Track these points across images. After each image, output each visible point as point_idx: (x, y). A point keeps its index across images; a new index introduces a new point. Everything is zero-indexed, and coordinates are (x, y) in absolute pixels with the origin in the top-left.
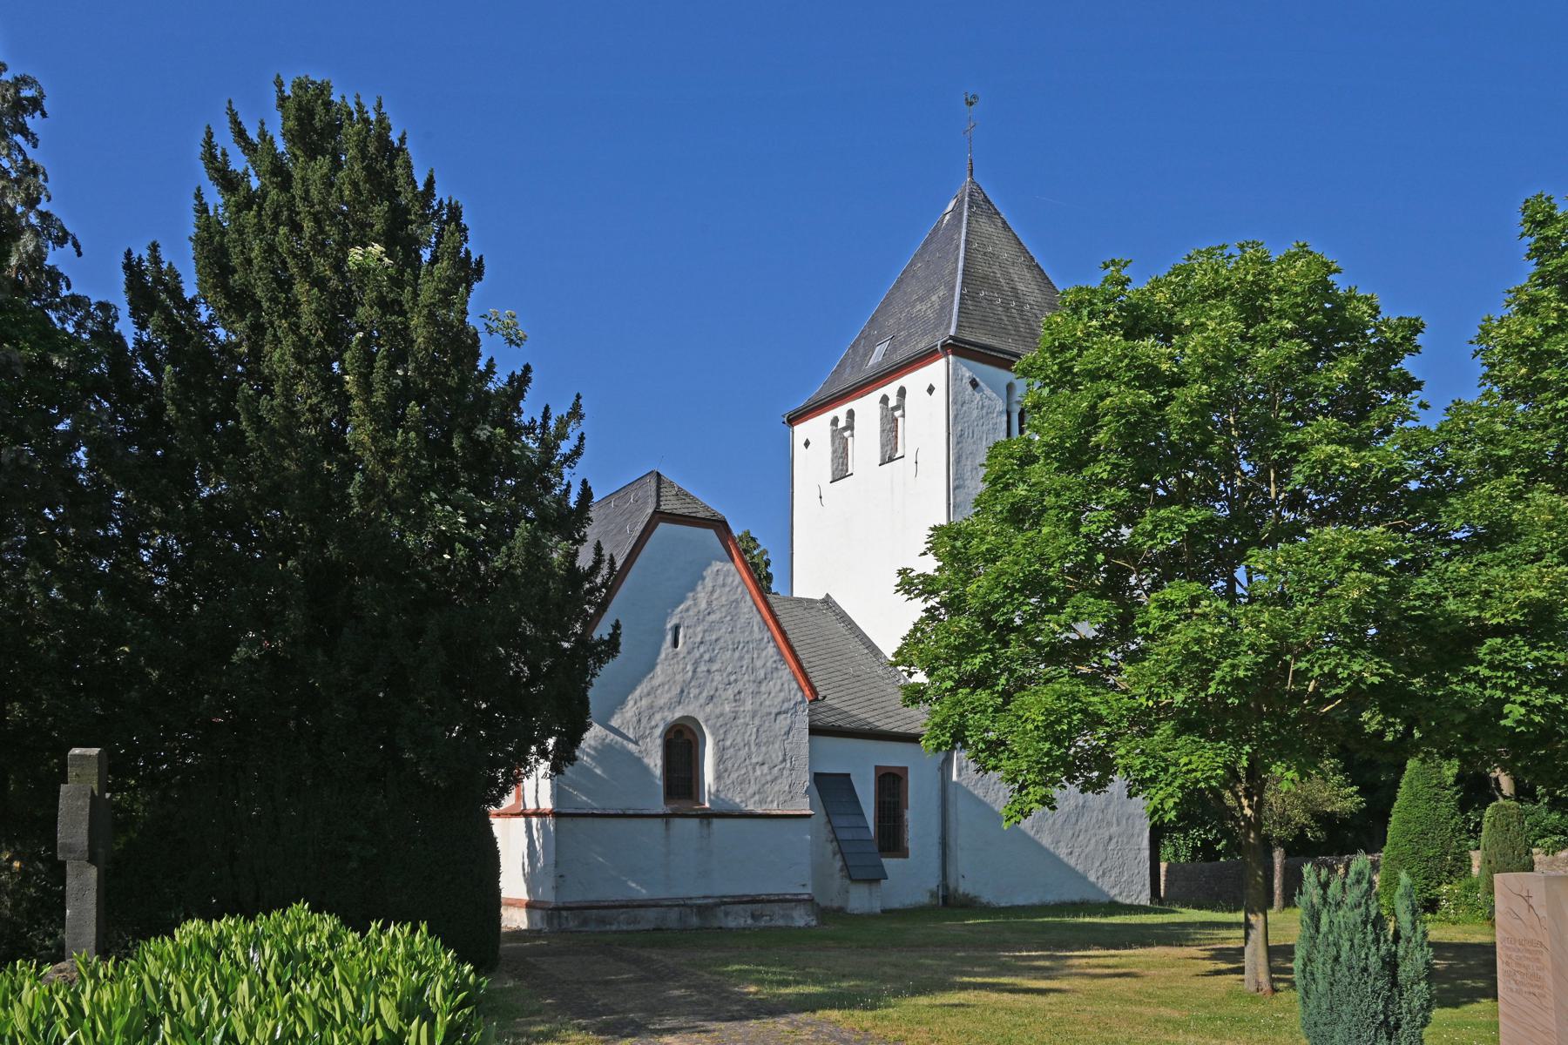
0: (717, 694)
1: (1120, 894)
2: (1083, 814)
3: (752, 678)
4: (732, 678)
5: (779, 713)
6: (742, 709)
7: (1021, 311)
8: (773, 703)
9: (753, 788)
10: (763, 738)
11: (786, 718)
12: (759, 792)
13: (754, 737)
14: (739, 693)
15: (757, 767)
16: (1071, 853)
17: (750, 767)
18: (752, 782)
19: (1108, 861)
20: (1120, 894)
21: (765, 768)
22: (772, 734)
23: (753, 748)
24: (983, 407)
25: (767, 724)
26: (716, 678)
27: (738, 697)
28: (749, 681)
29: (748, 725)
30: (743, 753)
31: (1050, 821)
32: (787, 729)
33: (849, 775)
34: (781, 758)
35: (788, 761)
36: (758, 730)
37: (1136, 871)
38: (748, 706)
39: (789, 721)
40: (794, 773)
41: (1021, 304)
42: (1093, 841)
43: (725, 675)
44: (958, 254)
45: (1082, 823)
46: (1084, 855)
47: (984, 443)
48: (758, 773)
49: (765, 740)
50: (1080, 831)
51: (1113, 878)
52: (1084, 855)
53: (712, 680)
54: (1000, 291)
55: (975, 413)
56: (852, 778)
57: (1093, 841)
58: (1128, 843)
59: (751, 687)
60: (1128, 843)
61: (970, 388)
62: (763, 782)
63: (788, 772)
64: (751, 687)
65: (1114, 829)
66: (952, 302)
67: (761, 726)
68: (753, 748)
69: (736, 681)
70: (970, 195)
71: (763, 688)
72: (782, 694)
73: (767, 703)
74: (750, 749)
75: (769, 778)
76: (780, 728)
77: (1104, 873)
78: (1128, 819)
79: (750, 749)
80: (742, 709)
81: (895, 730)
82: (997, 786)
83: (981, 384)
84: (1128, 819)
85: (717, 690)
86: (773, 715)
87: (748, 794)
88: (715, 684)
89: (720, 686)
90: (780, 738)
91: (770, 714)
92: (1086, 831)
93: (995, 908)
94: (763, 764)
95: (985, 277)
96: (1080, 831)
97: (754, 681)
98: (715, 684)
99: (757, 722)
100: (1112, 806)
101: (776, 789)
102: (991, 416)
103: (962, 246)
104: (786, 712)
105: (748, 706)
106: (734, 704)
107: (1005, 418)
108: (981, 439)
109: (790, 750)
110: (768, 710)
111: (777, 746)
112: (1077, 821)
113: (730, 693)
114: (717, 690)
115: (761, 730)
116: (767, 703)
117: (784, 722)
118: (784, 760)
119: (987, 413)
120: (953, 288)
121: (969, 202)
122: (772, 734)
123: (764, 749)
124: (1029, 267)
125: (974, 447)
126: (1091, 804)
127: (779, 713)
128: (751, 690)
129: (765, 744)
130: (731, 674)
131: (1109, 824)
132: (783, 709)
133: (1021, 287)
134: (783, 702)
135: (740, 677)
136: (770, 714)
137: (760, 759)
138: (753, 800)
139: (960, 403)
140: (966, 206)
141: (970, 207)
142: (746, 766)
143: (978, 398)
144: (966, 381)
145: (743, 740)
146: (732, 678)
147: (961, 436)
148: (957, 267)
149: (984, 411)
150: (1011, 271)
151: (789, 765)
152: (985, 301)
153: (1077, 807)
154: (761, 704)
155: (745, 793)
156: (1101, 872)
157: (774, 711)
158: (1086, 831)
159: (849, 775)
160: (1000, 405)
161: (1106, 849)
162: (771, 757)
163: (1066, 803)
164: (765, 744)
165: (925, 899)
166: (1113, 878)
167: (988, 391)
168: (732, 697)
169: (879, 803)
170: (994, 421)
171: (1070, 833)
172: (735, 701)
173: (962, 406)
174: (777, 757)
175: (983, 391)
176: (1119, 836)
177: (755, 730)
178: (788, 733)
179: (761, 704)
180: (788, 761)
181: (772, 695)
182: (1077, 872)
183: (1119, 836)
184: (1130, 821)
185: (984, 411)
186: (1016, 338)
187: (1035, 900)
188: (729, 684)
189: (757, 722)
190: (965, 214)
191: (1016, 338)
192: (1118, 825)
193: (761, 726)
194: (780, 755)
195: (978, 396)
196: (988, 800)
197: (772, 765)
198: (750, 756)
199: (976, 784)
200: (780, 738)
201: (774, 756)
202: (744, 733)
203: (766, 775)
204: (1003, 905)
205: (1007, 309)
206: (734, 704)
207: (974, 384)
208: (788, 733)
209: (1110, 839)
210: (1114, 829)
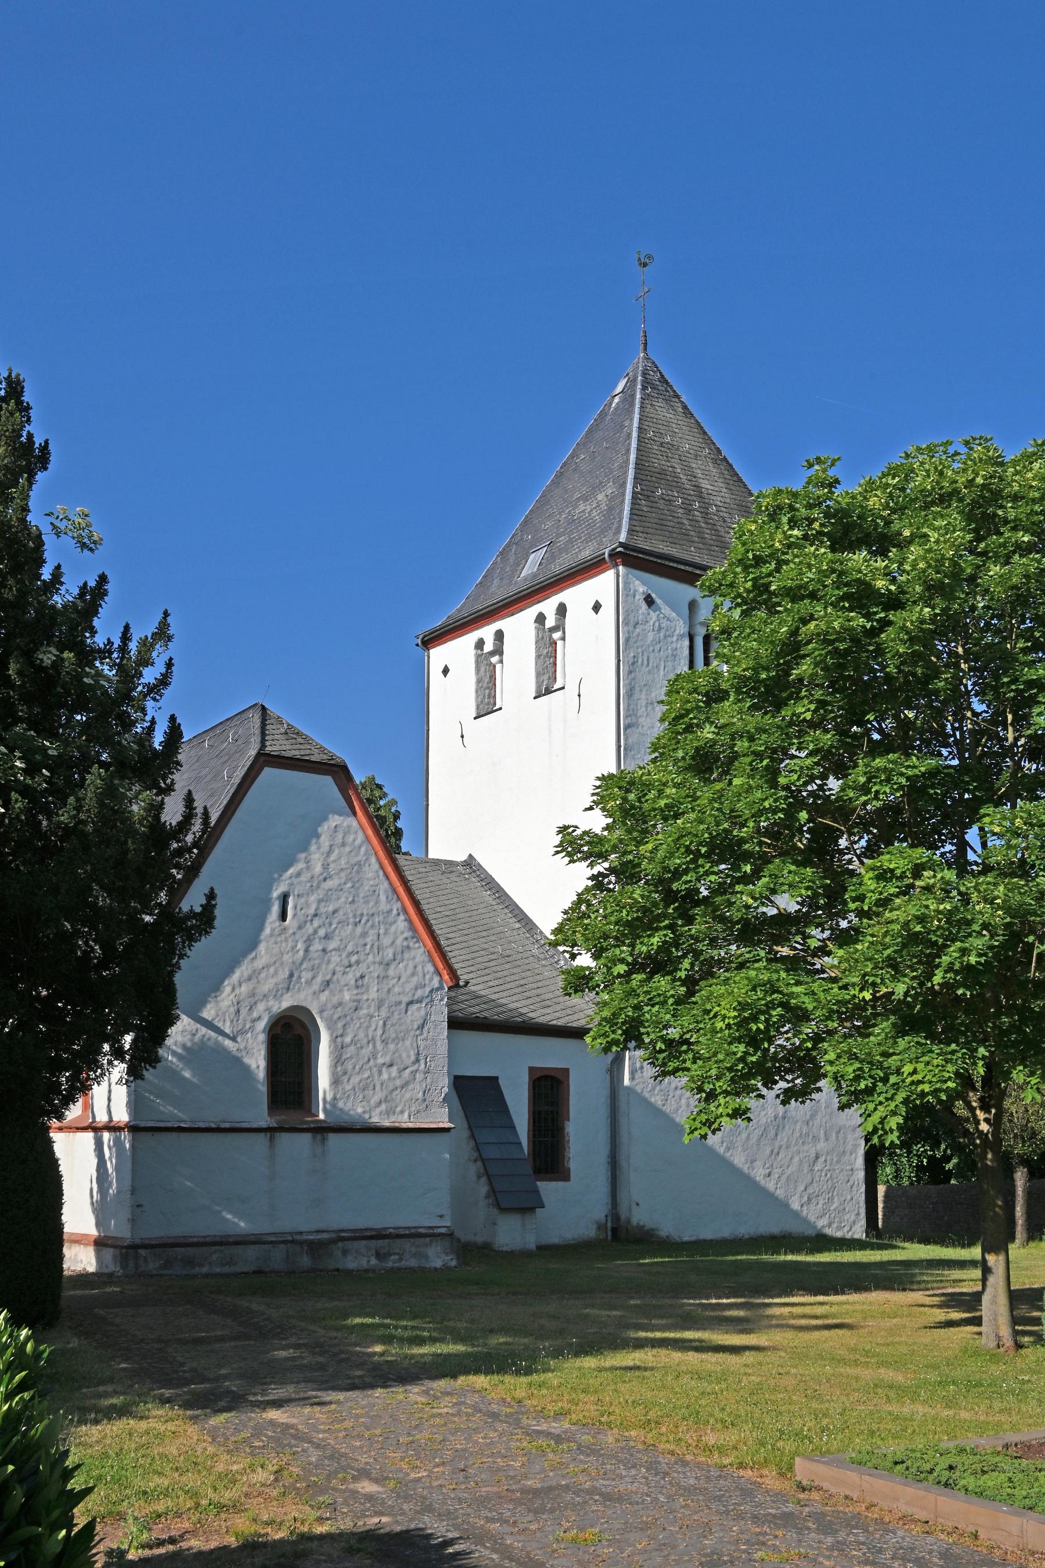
0: (335, 978)
1: (830, 1225)
2: (784, 1127)
3: (378, 959)
4: (354, 959)
5: (411, 1003)
6: (365, 997)
7: (706, 514)
8: (405, 991)
9: (379, 1095)
10: (391, 1033)
11: (419, 1009)
12: (386, 1101)
13: (379, 1032)
14: (362, 977)
15: (384, 1069)
16: (769, 1175)
17: (375, 1070)
18: (378, 1088)
19: (815, 1184)
20: (830, 1225)
21: (394, 1070)
22: (403, 1027)
23: (379, 1046)
24: (660, 629)
25: (396, 1016)
26: (333, 959)
27: (360, 983)
28: (374, 963)
29: (372, 1017)
30: (367, 1051)
31: (744, 1136)
32: (420, 1022)
33: (496, 1078)
34: (413, 1058)
35: (422, 1062)
36: (385, 1024)
37: (849, 1197)
38: (373, 994)
39: (423, 1013)
40: (429, 1076)
41: (705, 506)
42: (796, 1159)
43: (344, 955)
44: (630, 444)
45: (783, 1139)
46: (784, 1178)
48: (385, 1076)
49: (393, 1036)
51: (820, 1206)
52: (784, 1178)
53: (329, 962)
54: (680, 489)
55: (651, 636)
56: (500, 1081)
57: (796, 1159)
58: (838, 1162)
59: (377, 970)
60: (838, 1162)
61: (644, 606)
62: (391, 1087)
63: (422, 1075)
64: (377, 970)
65: (821, 1145)
66: (623, 501)
67: (388, 1018)
68: (379, 1046)
69: (358, 962)
70: (644, 374)
71: (391, 972)
72: (415, 979)
73: (397, 989)
74: (374, 1047)
75: (398, 1082)
76: (412, 1021)
77: (809, 1200)
78: (838, 1133)
79: (374, 1047)
80: (365, 997)
81: (554, 1022)
82: (679, 1092)
83: (658, 601)
84: (838, 1133)
85: (334, 974)
86: (403, 1006)
87: (372, 1101)
88: (331, 966)
89: (338, 969)
90: (412, 1033)
91: (400, 1003)
92: (788, 1147)
93: (676, 1243)
94: (391, 1065)
95: (662, 472)
97: (381, 963)
98: (331, 966)
99: (384, 1013)
100: (819, 1117)
101: (408, 1095)
103: (635, 434)
104: (419, 1001)
105: (373, 994)
106: (355, 992)
107: (687, 643)
109: (426, 1047)
110: (398, 1000)
111: (408, 1043)
112: (776, 1135)
113: (351, 977)
114: (334, 974)
115: (389, 1023)
116: (397, 989)
117: (416, 1014)
118: (417, 1060)
119: (665, 637)
120: (624, 485)
121: (643, 381)
122: (403, 1027)
123: (392, 1046)
124: (715, 461)
126: (794, 1113)
127: (411, 1003)
128: (376, 975)
129: (393, 1041)
130: (352, 953)
132: (416, 997)
133: (705, 485)
134: (416, 989)
135: (362, 957)
136: (400, 1003)
137: (387, 1059)
138: (378, 1110)
139: (632, 623)
140: (639, 386)
141: (644, 388)
142: (370, 1068)
143: (654, 619)
144: (640, 597)
145: (367, 1036)
146: (354, 959)
147: (633, 664)
148: (628, 460)
150: (694, 465)
151: (423, 1066)
152: (662, 501)
153: (776, 1118)
154: (389, 991)
155: (369, 1102)
156: (806, 1199)
157: (405, 999)
159: (496, 1078)
160: (681, 627)
162: (400, 1056)
163: (763, 1113)
164: (393, 1041)
166: (820, 1206)
168: (353, 982)
169: (534, 1114)
170: (674, 645)
172: (357, 987)
173: (635, 627)
174: (408, 1056)
175: (659, 609)
176: (828, 1154)
177: (381, 1023)
178: (422, 1027)
179: (389, 991)
180: (422, 1062)
181: (402, 980)
182: (777, 1199)
183: (828, 1154)
184: (841, 1135)
186: (700, 546)
187: (726, 1233)
188: (350, 966)
189: (384, 1013)
190: (638, 396)
191: (700, 546)
192: (827, 1140)
193: (388, 1018)
194: (412, 1053)
195: (653, 616)
196: (667, 1109)
197: (402, 1067)
198: (374, 1056)
199: (653, 1089)
200: (412, 1033)
201: (404, 1055)
202: (368, 1027)
203: (394, 1079)
204: (686, 1239)
205: (689, 511)
206: (355, 992)
207: (649, 601)
208: (422, 1027)
209: (817, 1157)
210: (821, 1145)
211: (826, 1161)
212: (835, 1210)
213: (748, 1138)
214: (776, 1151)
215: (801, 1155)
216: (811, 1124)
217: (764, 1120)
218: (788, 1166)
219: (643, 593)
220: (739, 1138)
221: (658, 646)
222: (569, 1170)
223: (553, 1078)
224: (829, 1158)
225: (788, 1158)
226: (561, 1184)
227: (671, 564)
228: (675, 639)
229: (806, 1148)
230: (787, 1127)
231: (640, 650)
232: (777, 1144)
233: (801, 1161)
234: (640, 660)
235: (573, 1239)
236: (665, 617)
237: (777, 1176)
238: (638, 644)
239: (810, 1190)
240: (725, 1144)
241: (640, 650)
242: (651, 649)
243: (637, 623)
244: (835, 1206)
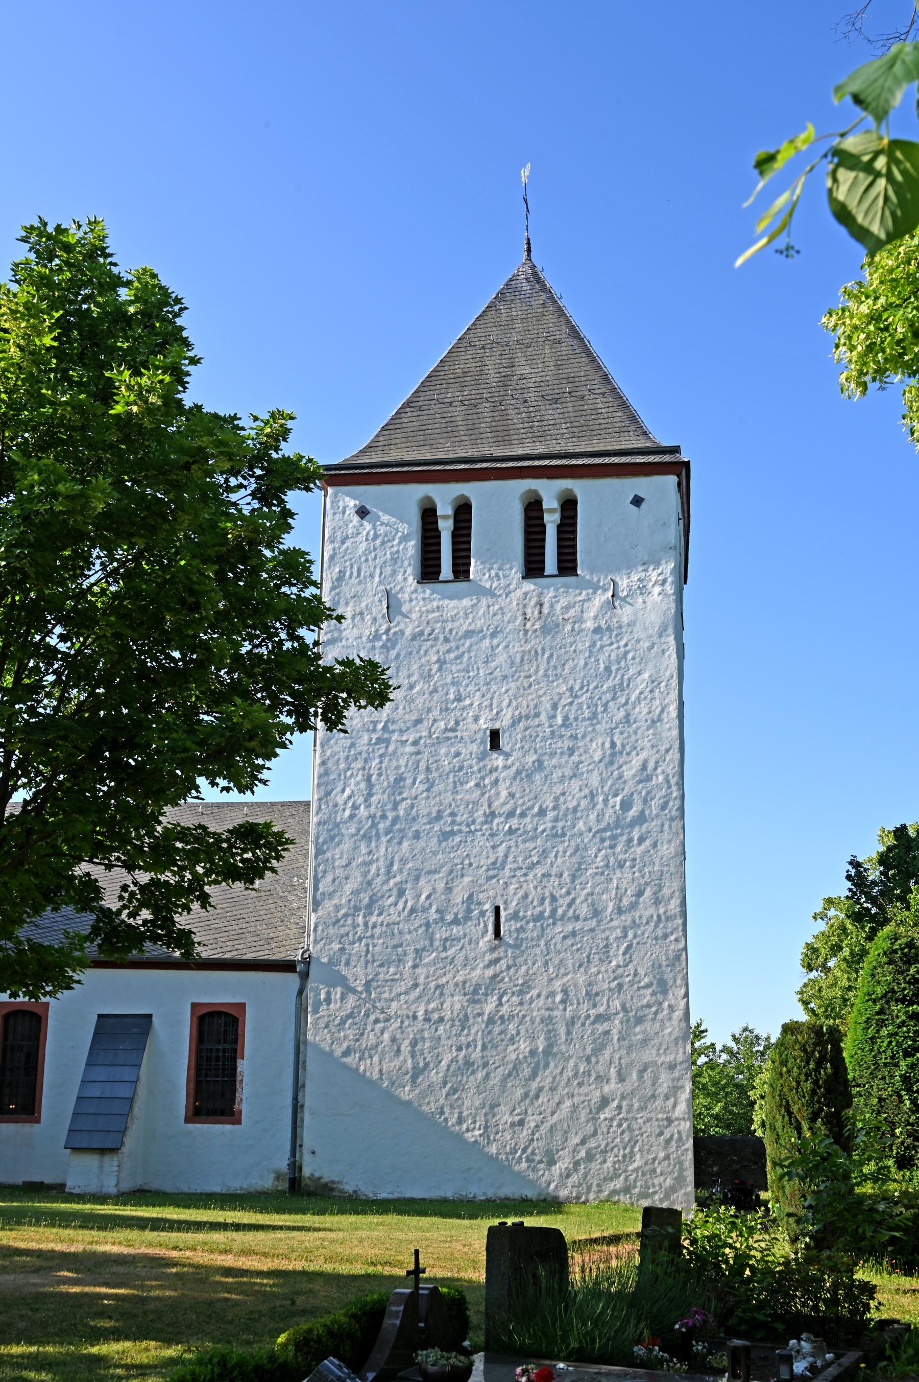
2: (547, 1065)
16: (521, 1123)
24: (376, 536)
31: (480, 1075)
37: (661, 1155)
42: (568, 1103)
45: (545, 1079)
46: (547, 1126)
47: (377, 579)
50: (541, 1089)
51: (609, 1164)
52: (547, 1126)
55: (363, 547)
57: (568, 1103)
58: (641, 1109)
60: (641, 1109)
65: (612, 1087)
77: (590, 1157)
78: (641, 1072)
82: (379, 1026)
84: (641, 1072)
92: (553, 1089)
96: (541, 1089)
100: (607, 1054)
102: (390, 544)
108: (372, 576)
119: (383, 543)
125: (360, 588)
131: (601, 1079)
139: (339, 539)
147: (338, 579)
149: (378, 542)
156: (583, 1154)
158: (553, 1089)
161: (594, 1119)
163: (511, 1048)
165: (268, 1183)
166: (609, 1164)
167: (385, 518)
171: (519, 1093)
176: (623, 1097)
183: (623, 1097)
184: (647, 1076)
185: (378, 542)
187: (448, 1192)
192: (621, 1079)
195: (367, 526)
207: (362, 512)
209: (605, 1102)
210: (612, 1087)
211: (619, 1107)
212: (636, 1170)
213: (487, 1076)
214: (532, 1094)
215: (576, 1100)
216: (594, 1060)
217: (513, 1056)
218: (553, 1113)
219: (355, 505)
220: (471, 1078)
221: (373, 554)
222: (240, 1112)
223: (227, 1015)
224: (624, 1103)
225: (553, 1103)
226: (228, 1127)
227: (342, 472)
228: (396, 542)
229: (584, 1089)
230: (552, 1065)
231: (348, 563)
232: (534, 1085)
233: (575, 1107)
234: (348, 574)
235: (241, 1189)
236: (382, 524)
237: (533, 1124)
238: (346, 558)
239: (592, 1144)
240: (449, 1085)
241: (348, 563)
242: (363, 559)
243: (347, 537)
244: (635, 1165)
